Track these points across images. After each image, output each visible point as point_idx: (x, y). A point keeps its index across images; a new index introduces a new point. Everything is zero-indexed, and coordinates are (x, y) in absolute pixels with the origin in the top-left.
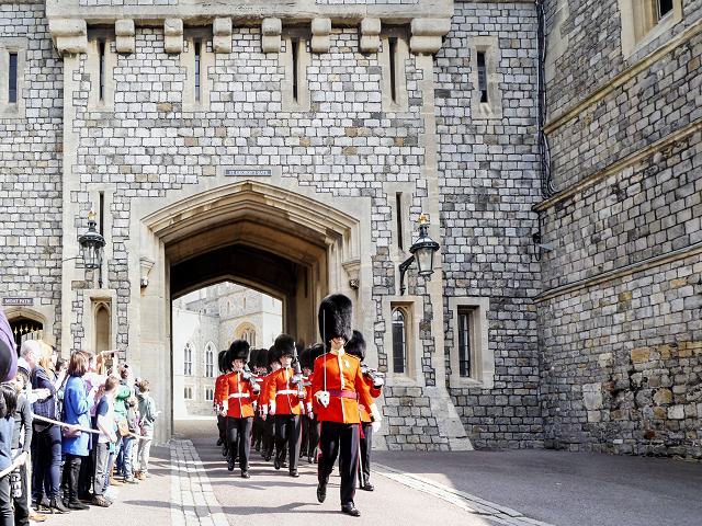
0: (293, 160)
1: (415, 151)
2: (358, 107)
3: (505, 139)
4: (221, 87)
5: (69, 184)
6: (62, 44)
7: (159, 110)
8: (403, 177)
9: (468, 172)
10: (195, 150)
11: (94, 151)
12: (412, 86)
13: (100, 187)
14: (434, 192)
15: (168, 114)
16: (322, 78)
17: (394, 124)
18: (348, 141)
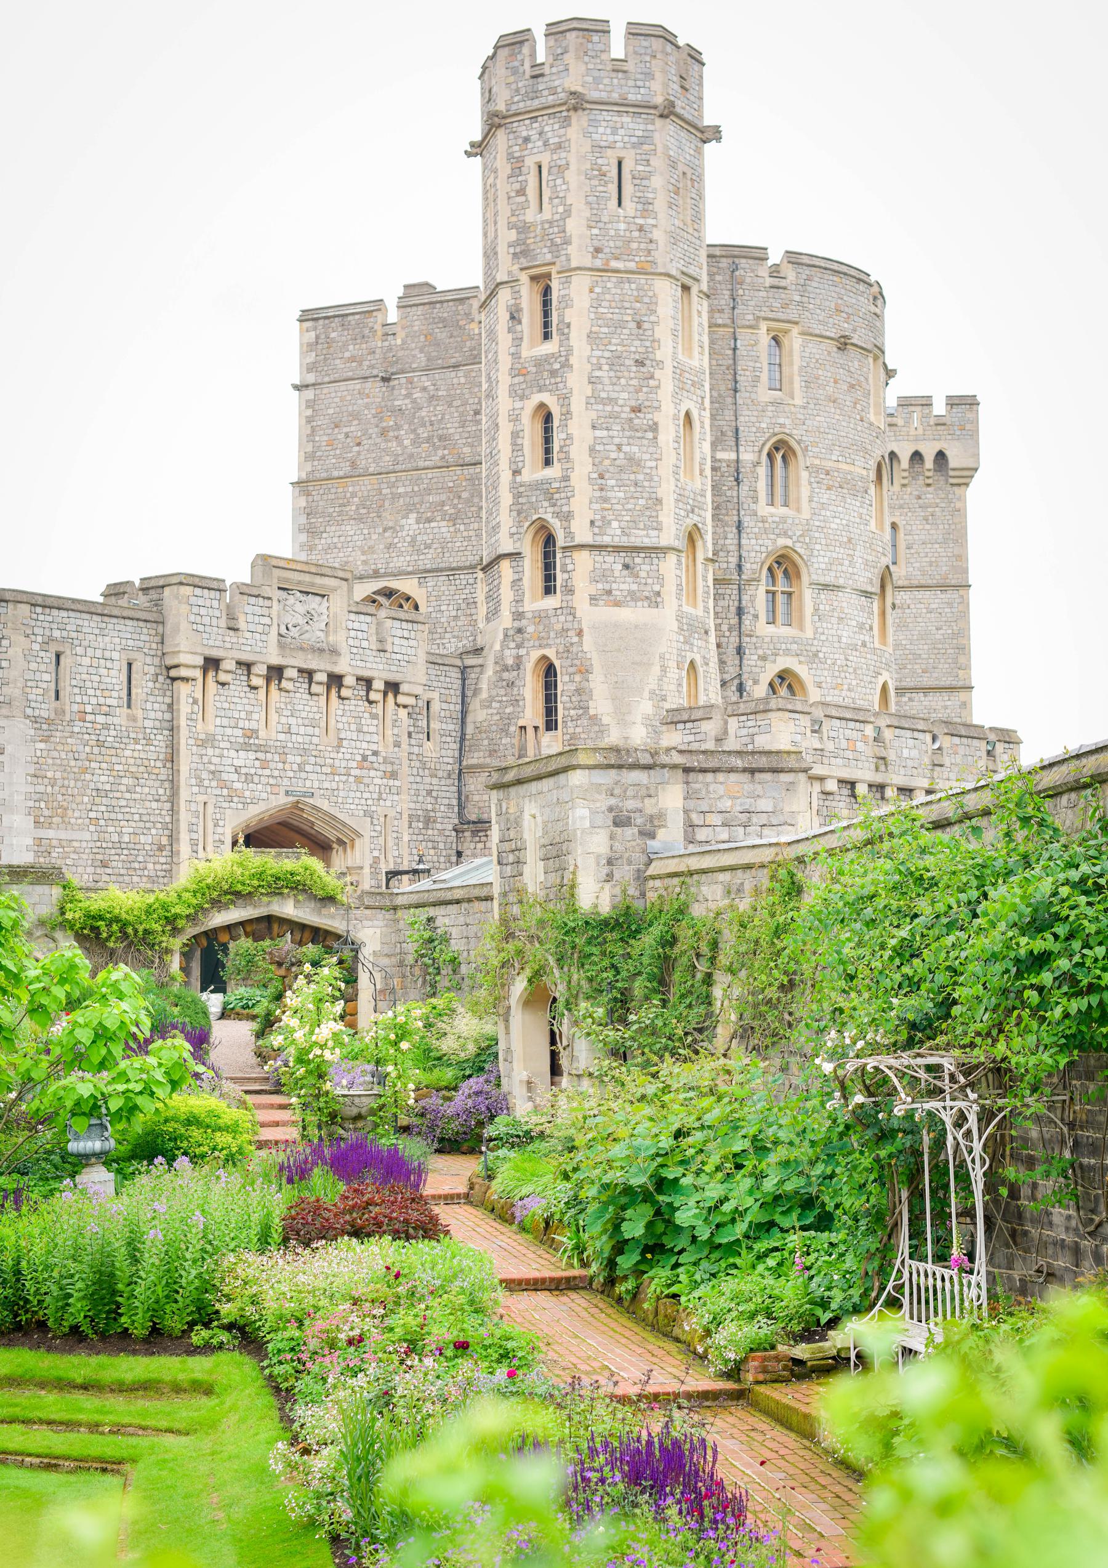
0: (326, 785)
1: (397, 783)
2: (365, 745)
3: (440, 774)
4: (283, 720)
5: (184, 794)
6: (183, 672)
7: (245, 736)
8: (388, 803)
9: (420, 799)
10: (267, 772)
11: (200, 766)
12: (396, 731)
13: (201, 798)
14: (405, 816)
15: (249, 741)
16: (344, 719)
17: (385, 761)
18: (357, 772)
